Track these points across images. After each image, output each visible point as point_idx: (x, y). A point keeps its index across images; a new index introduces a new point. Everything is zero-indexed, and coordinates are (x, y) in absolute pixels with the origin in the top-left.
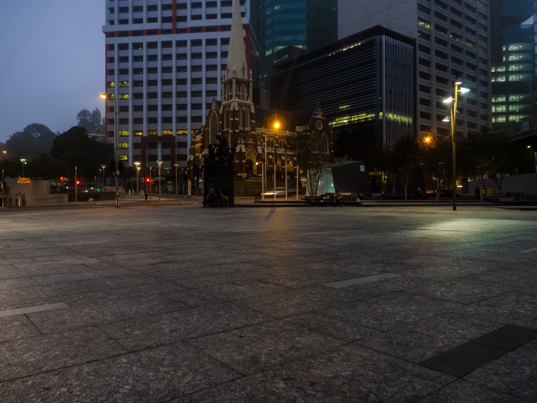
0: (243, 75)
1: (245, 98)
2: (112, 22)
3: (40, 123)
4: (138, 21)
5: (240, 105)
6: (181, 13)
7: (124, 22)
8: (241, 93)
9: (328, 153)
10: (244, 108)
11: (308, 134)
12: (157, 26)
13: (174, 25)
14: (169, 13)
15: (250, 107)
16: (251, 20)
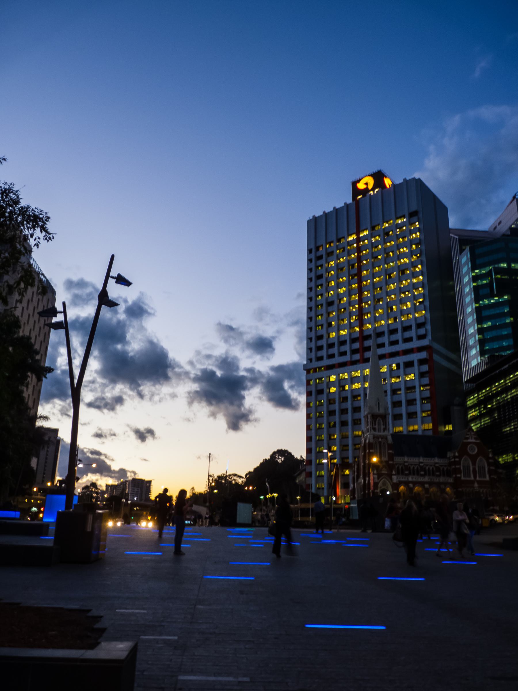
0: (379, 410)
1: (382, 430)
2: (310, 360)
3: (283, 449)
4: (332, 356)
5: (375, 437)
6: (367, 343)
7: (320, 359)
8: (377, 427)
9: (487, 478)
10: (380, 440)
11: (457, 459)
12: (346, 358)
13: (362, 356)
14: (357, 345)
15: (386, 438)
16: (434, 339)
